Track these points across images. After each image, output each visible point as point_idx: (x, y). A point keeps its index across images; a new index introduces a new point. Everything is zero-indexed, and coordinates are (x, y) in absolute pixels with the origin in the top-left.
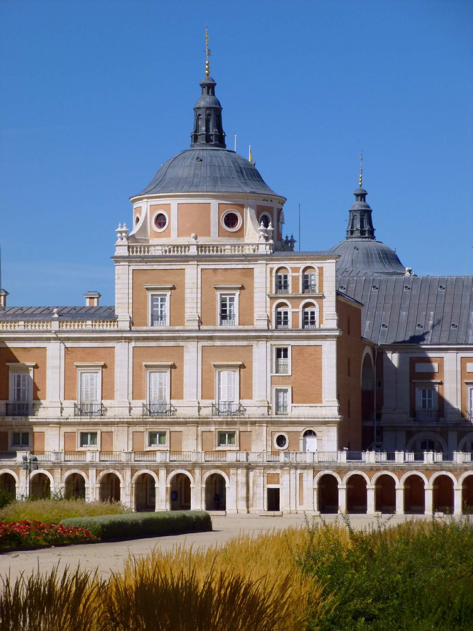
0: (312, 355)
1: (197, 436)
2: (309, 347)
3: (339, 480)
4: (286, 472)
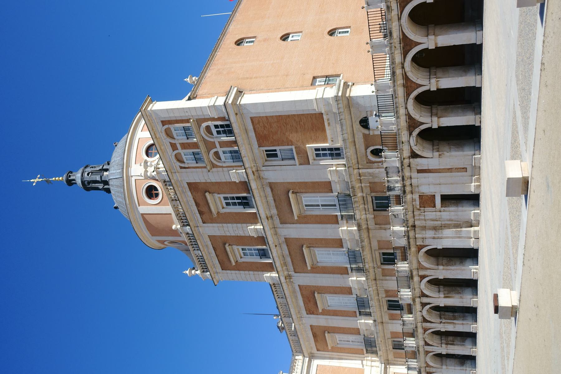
0: (265, 127)
1: (381, 228)
2: (257, 130)
3: (423, 127)
4: (417, 190)
